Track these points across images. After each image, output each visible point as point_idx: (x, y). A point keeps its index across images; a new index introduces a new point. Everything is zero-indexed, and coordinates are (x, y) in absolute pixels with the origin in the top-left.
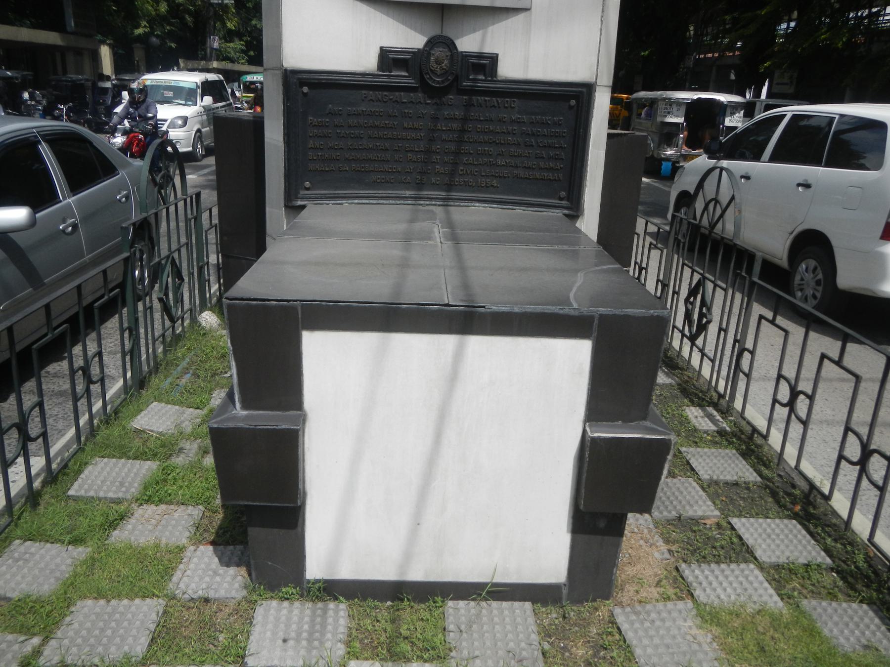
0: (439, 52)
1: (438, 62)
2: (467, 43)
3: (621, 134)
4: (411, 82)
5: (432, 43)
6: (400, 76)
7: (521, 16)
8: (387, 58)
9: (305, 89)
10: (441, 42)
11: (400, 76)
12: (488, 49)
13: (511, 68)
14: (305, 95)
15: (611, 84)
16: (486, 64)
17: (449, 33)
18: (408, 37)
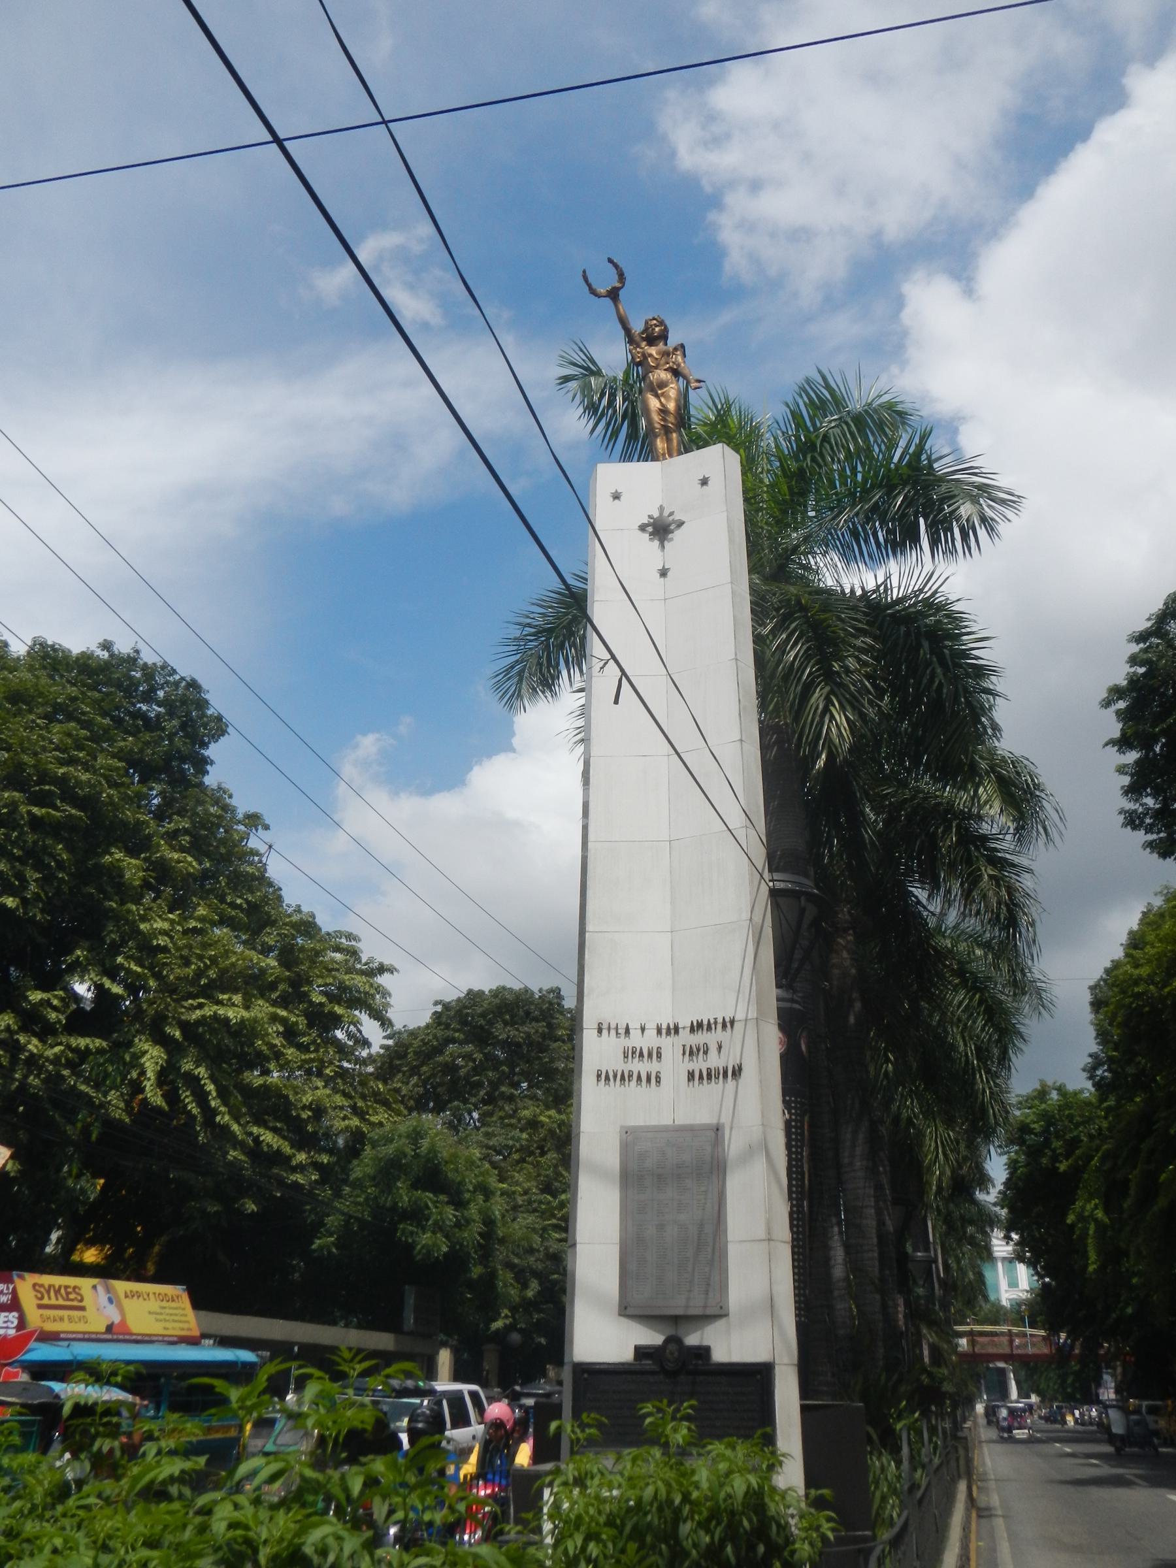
0: (672, 1347)
1: (672, 1353)
2: (692, 1340)
3: (837, 1406)
4: (655, 1368)
5: (666, 1341)
6: (648, 1363)
7: (724, 1320)
8: (640, 1352)
9: (586, 1376)
10: (673, 1340)
11: (648, 1363)
12: (705, 1343)
13: (722, 1354)
14: (585, 1379)
15: (795, 1361)
16: (703, 1352)
17: (680, 1333)
18: (653, 1338)
